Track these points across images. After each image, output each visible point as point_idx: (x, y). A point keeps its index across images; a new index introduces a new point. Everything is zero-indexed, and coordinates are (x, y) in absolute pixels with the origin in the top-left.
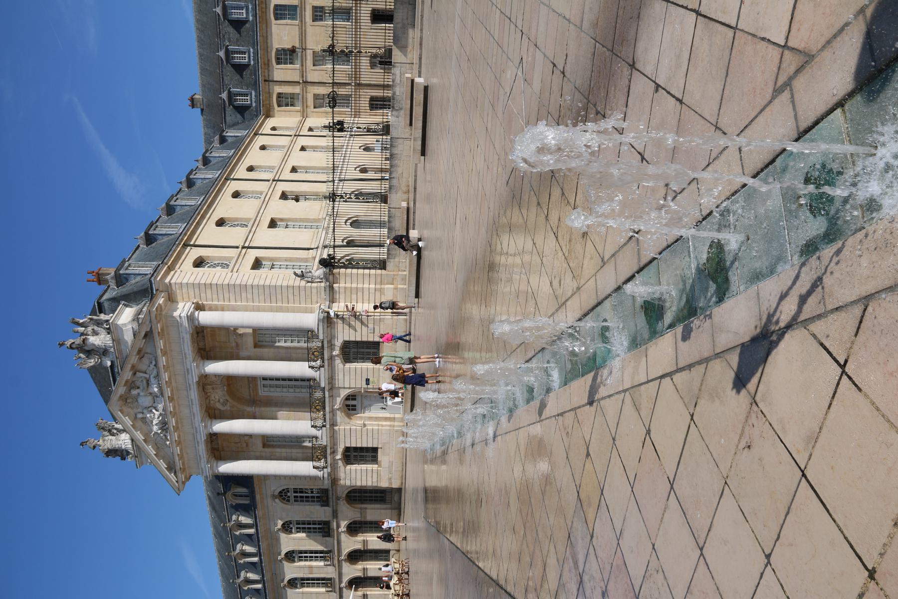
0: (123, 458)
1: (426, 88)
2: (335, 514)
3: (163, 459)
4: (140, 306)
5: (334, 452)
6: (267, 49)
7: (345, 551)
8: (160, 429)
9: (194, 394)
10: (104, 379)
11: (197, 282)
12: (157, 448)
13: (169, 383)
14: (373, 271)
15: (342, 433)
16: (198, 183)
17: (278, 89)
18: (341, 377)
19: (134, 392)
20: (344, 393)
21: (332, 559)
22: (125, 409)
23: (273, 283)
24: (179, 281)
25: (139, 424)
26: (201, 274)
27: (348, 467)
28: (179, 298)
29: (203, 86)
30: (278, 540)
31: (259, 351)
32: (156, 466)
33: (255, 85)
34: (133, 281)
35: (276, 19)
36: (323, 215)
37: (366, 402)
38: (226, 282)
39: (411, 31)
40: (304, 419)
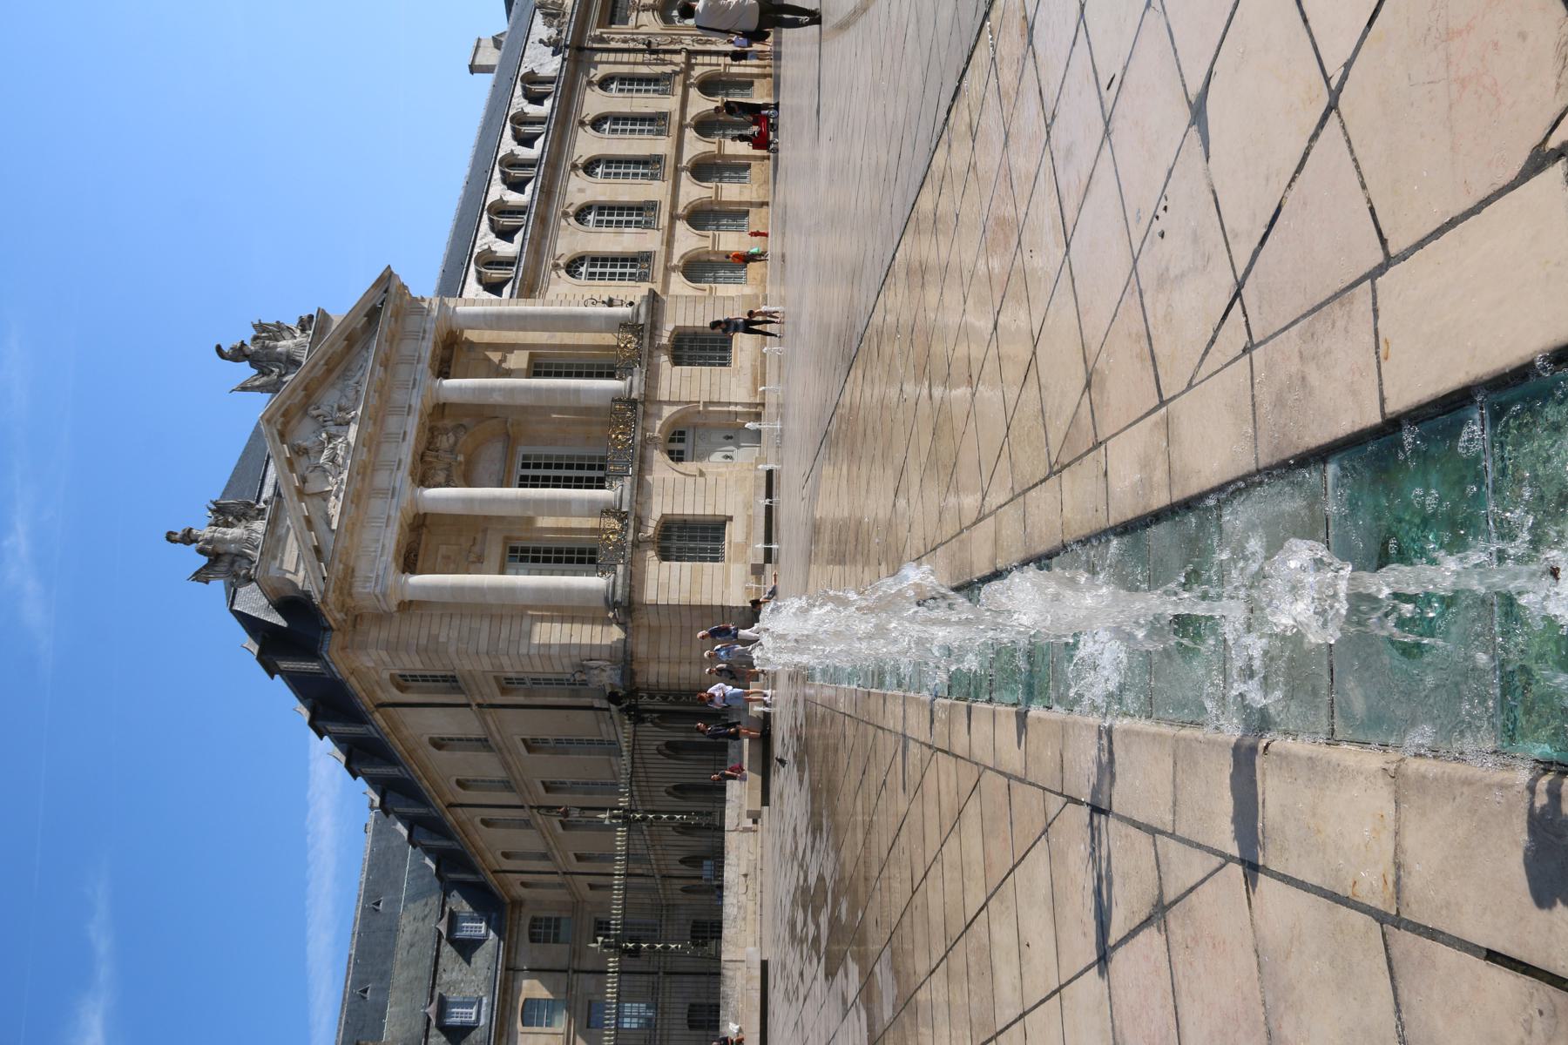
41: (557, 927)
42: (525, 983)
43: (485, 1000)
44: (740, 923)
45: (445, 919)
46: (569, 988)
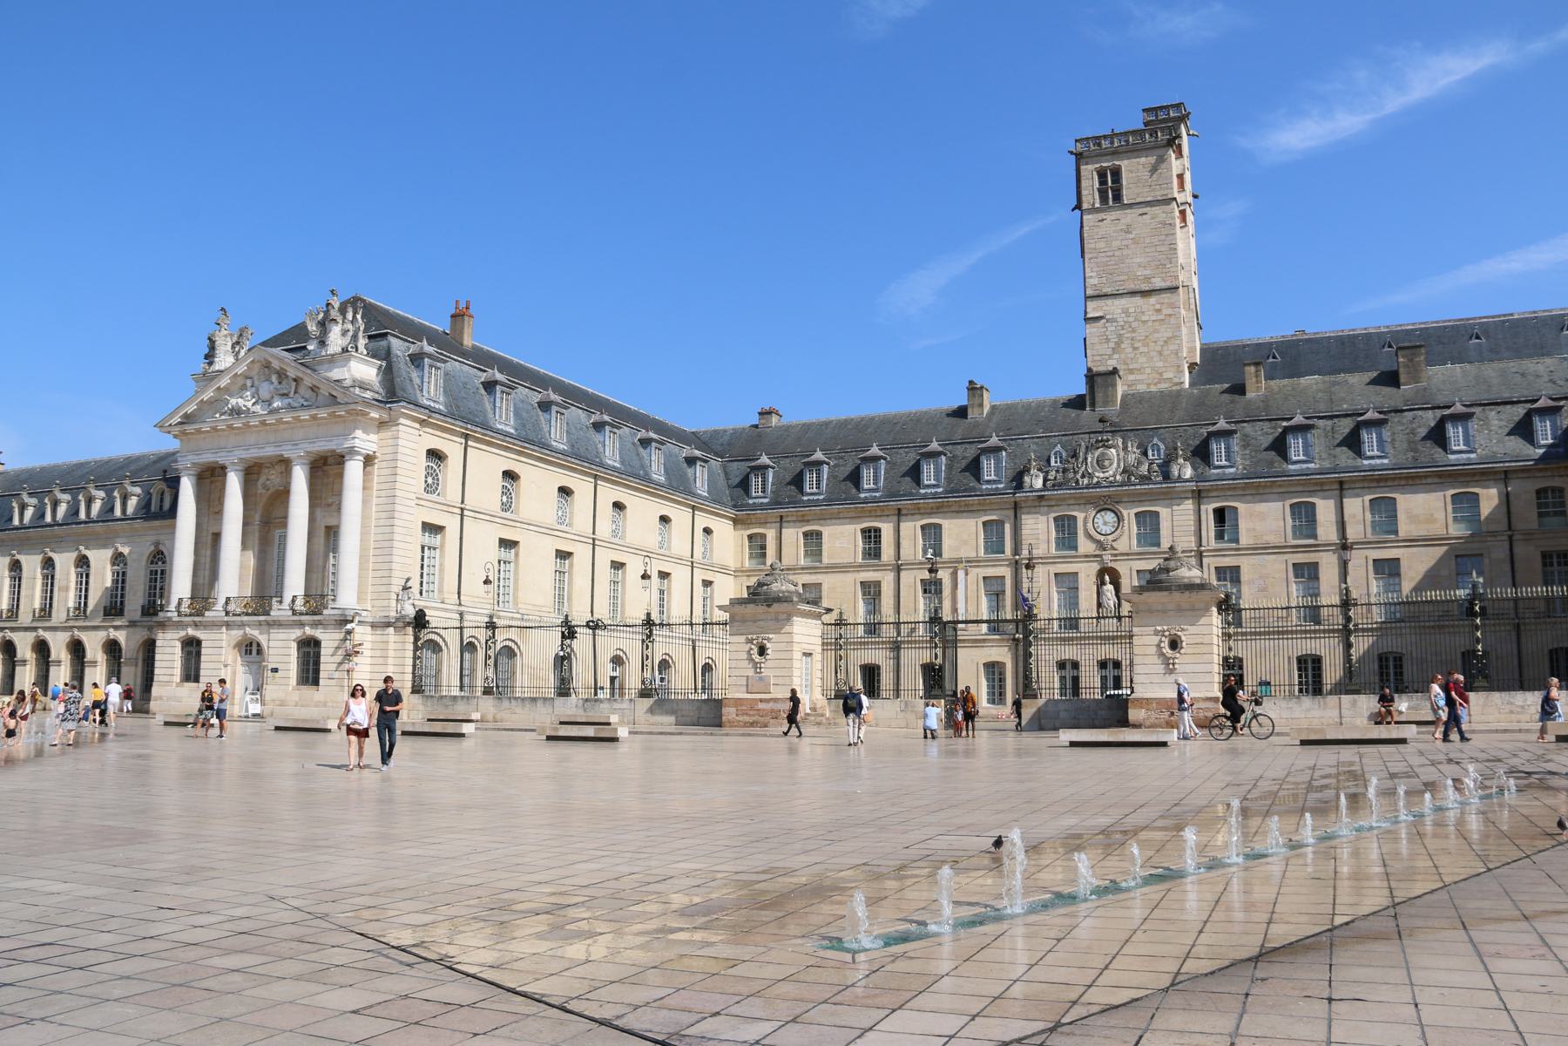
0: (206, 357)
1: (614, 740)
2: (133, 624)
3: (199, 409)
4: (377, 387)
5: (196, 625)
6: (822, 518)
7: (85, 637)
8: (232, 410)
9: (270, 451)
10: (294, 339)
11: (400, 456)
12: (211, 402)
13: (280, 421)
14: (410, 677)
15: (217, 636)
16: (597, 437)
17: (771, 534)
18: (282, 636)
19: (274, 378)
20: (263, 639)
21: (76, 618)
22: (257, 366)
23: (395, 551)
24: (401, 435)
25: (240, 381)
26: (414, 460)
27: (179, 644)
28: (383, 435)
29: (787, 428)
30: (105, 546)
31: (321, 533)
32: (189, 401)
33: (776, 503)
34: (415, 375)
35: (863, 531)
36: (523, 608)
37: (255, 667)
38: (398, 493)
39: (672, 719)
40: (240, 588)
41: (1556, 514)
42: (1494, 492)
43: (1473, 456)
44: (1508, 707)
45: (1551, 403)
46: (1493, 534)
